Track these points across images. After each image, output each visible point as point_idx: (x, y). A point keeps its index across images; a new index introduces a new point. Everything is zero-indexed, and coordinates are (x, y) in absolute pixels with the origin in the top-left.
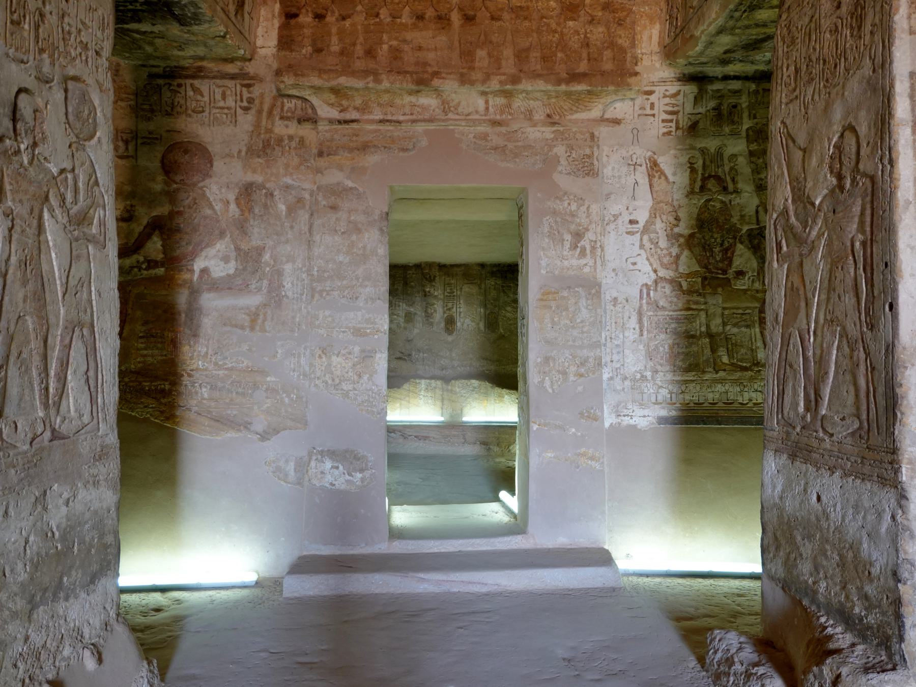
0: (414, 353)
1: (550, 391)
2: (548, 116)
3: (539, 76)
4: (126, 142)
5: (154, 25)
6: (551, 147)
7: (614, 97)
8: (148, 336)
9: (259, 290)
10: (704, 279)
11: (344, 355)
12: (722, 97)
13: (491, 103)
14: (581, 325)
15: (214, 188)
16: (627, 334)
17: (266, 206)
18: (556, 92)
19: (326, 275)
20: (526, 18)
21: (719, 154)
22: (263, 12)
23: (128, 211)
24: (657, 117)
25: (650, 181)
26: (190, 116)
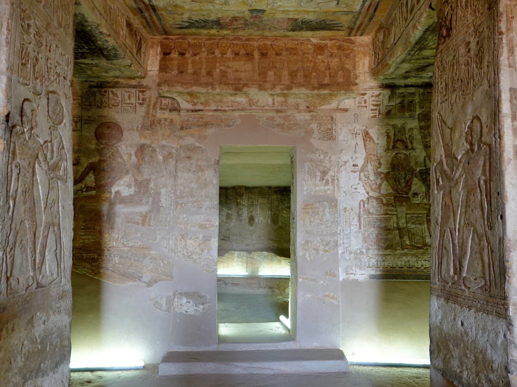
0: (231, 237)
1: (309, 259)
2: (307, 107)
3: (303, 86)
4: (76, 122)
5: (93, 60)
6: (309, 124)
7: (344, 97)
8: (86, 228)
9: (147, 203)
10: (395, 197)
11: (194, 239)
12: (404, 97)
13: (276, 100)
14: (326, 223)
15: (123, 147)
16: (352, 228)
17: (151, 157)
18: (312, 94)
19: (184, 195)
20: (295, 54)
21: (403, 128)
22: (151, 52)
24: (368, 107)
25: (364, 143)
26: (111, 108)
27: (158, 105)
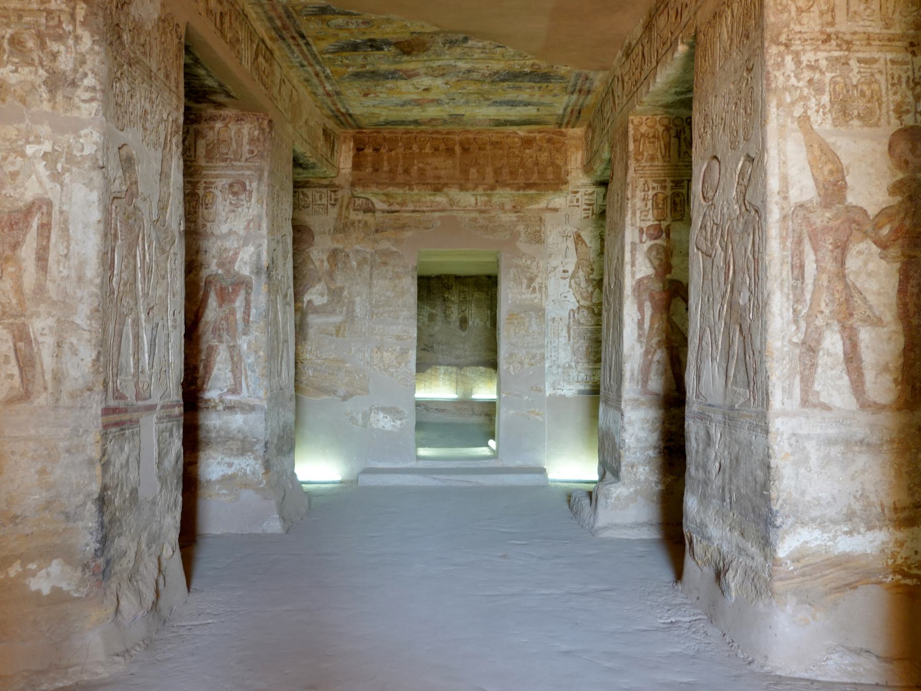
2: (514, 207)
6: (515, 226)
15: (315, 252)
17: (345, 263)
22: (343, 148)
27: (351, 206)
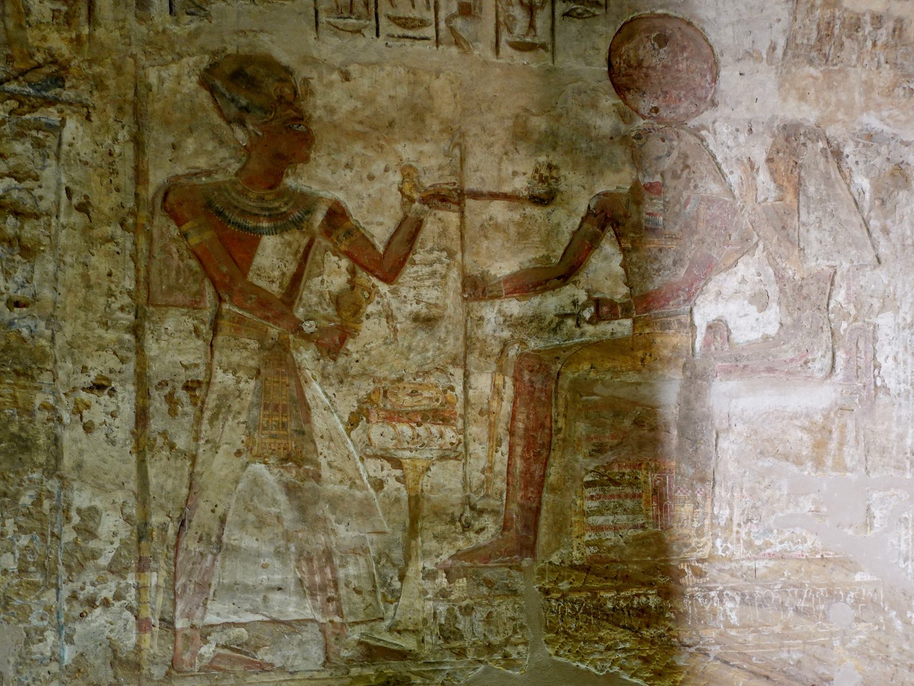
15: (723, 129)
23: (543, 180)
